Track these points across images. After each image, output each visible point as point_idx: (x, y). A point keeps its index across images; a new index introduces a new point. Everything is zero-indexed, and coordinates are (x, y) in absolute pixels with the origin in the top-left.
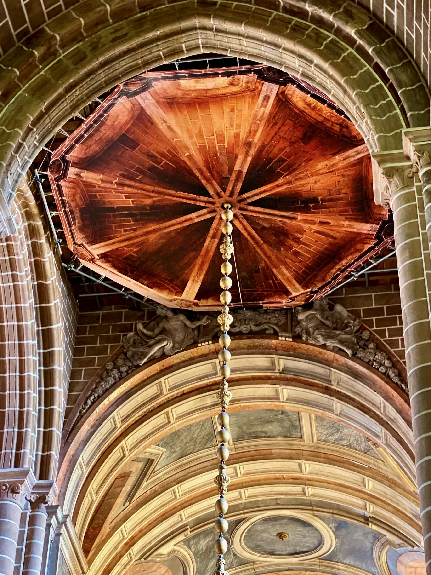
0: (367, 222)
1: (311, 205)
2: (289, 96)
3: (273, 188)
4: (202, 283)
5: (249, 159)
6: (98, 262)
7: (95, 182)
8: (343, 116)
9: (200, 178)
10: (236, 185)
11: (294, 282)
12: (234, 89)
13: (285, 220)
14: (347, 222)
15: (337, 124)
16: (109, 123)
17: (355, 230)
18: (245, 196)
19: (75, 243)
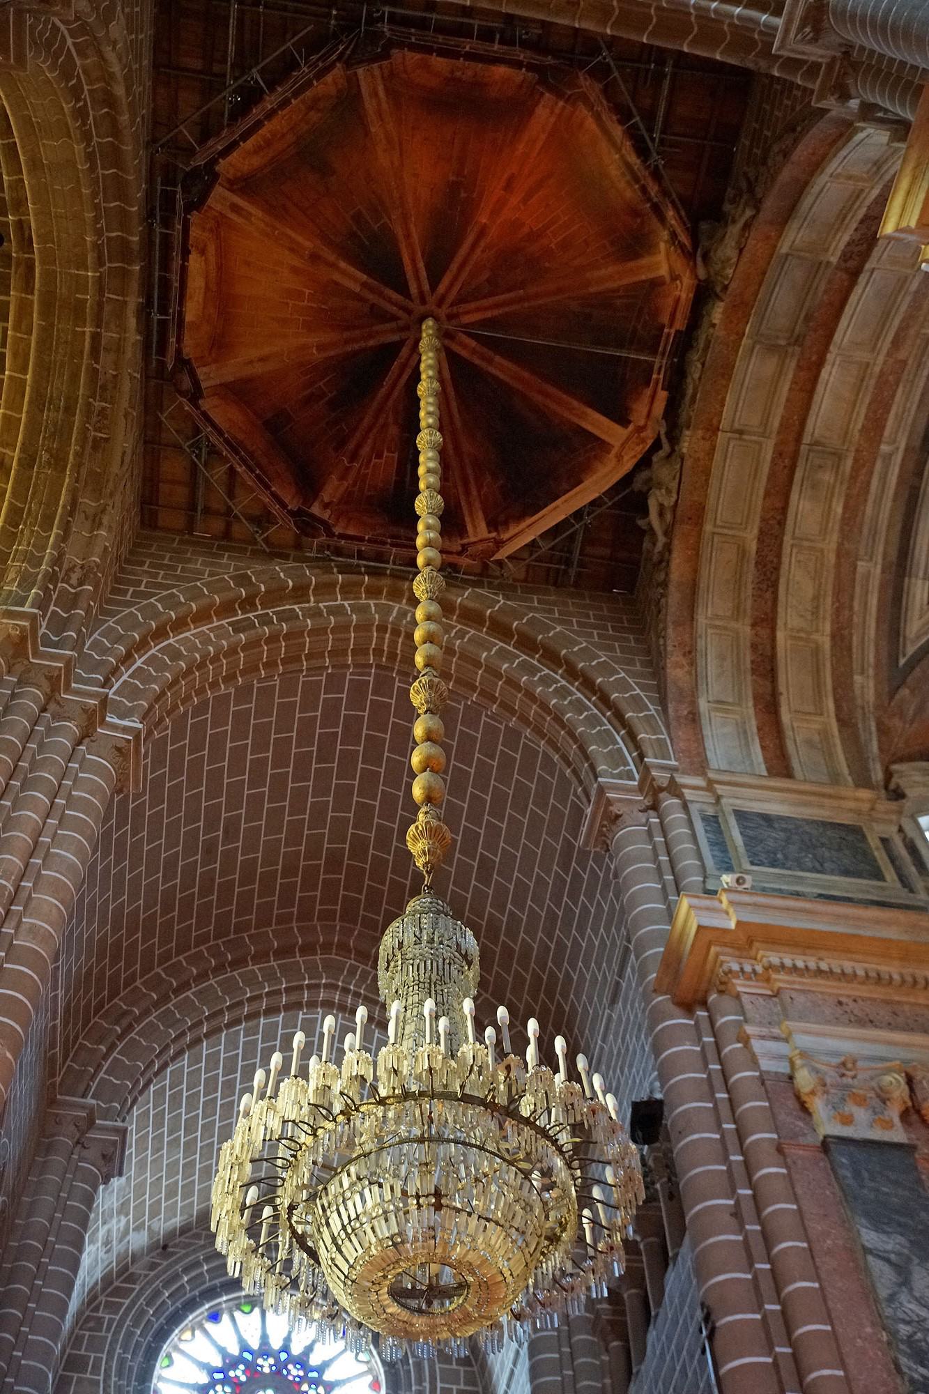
0: (531, 113)
1: (463, 195)
2: (239, 174)
3: (410, 246)
4: (590, 407)
5: (343, 264)
6: (505, 536)
7: (342, 489)
8: (293, 101)
9: (363, 344)
10: (390, 298)
11: (632, 264)
12: (211, 249)
13: (482, 244)
14: (521, 147)
15: (307, 114)
16: (241, 436)
17: (543, 137)
18: (413, 290)
19: (459, 554)
